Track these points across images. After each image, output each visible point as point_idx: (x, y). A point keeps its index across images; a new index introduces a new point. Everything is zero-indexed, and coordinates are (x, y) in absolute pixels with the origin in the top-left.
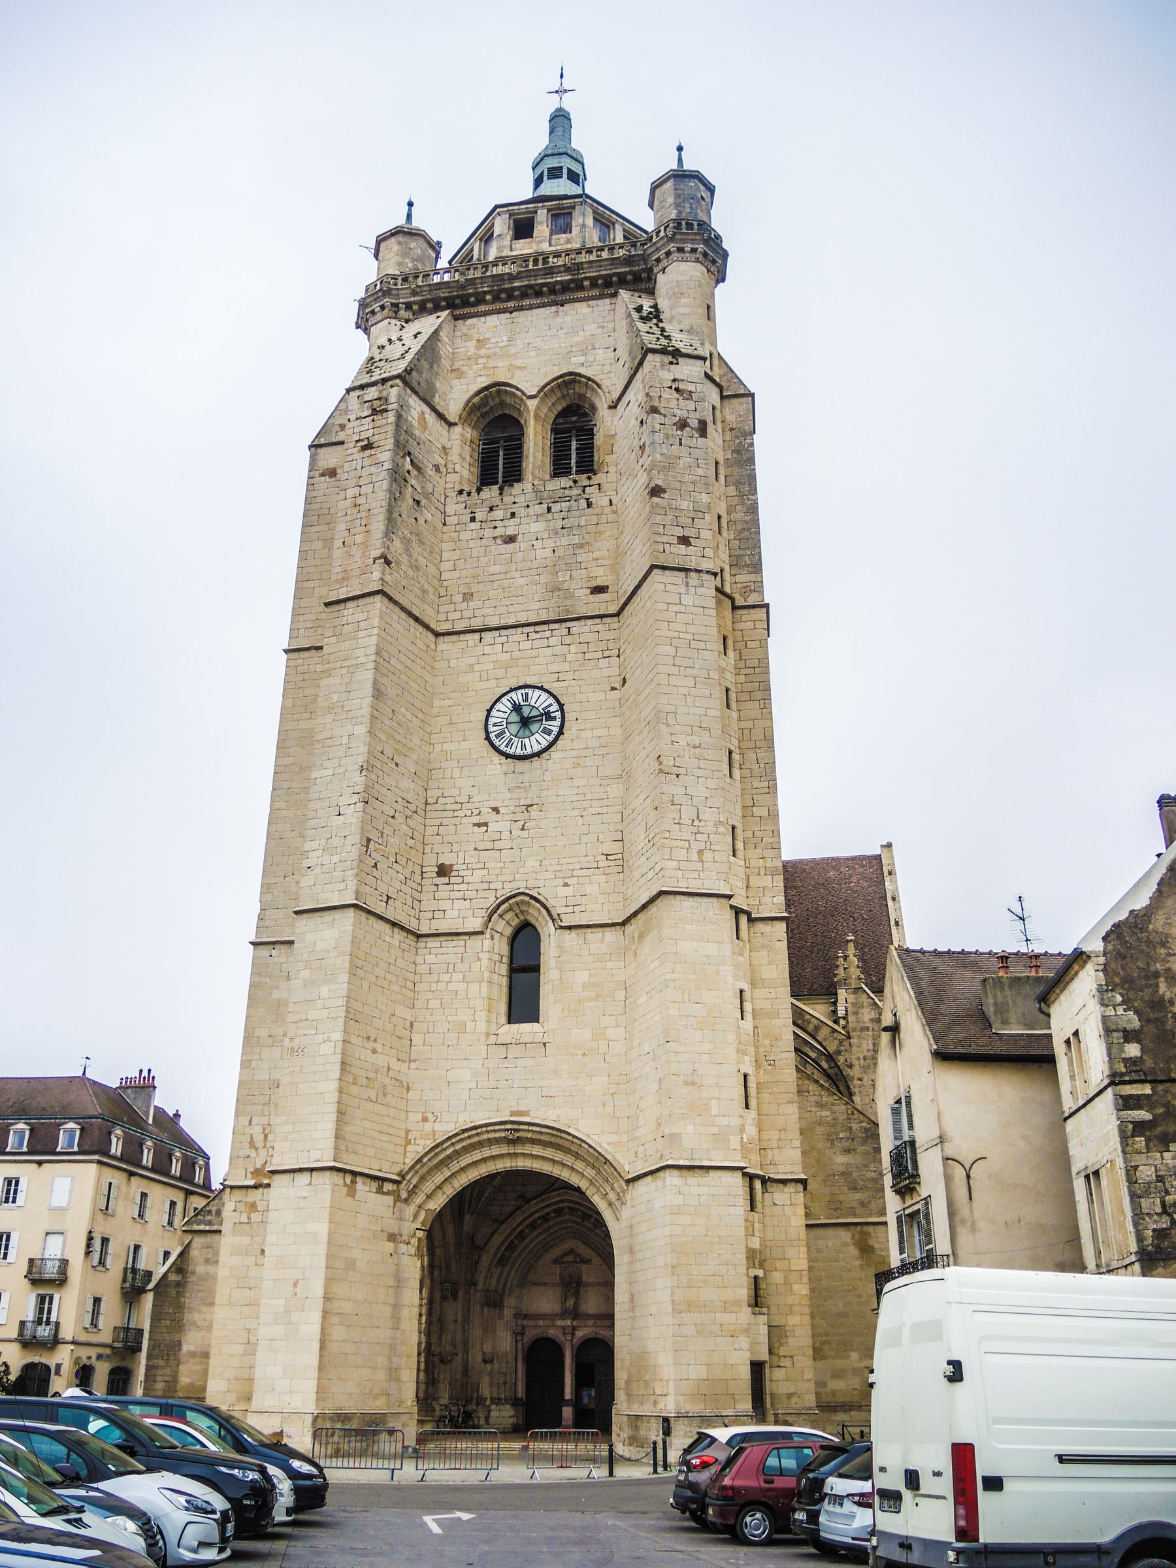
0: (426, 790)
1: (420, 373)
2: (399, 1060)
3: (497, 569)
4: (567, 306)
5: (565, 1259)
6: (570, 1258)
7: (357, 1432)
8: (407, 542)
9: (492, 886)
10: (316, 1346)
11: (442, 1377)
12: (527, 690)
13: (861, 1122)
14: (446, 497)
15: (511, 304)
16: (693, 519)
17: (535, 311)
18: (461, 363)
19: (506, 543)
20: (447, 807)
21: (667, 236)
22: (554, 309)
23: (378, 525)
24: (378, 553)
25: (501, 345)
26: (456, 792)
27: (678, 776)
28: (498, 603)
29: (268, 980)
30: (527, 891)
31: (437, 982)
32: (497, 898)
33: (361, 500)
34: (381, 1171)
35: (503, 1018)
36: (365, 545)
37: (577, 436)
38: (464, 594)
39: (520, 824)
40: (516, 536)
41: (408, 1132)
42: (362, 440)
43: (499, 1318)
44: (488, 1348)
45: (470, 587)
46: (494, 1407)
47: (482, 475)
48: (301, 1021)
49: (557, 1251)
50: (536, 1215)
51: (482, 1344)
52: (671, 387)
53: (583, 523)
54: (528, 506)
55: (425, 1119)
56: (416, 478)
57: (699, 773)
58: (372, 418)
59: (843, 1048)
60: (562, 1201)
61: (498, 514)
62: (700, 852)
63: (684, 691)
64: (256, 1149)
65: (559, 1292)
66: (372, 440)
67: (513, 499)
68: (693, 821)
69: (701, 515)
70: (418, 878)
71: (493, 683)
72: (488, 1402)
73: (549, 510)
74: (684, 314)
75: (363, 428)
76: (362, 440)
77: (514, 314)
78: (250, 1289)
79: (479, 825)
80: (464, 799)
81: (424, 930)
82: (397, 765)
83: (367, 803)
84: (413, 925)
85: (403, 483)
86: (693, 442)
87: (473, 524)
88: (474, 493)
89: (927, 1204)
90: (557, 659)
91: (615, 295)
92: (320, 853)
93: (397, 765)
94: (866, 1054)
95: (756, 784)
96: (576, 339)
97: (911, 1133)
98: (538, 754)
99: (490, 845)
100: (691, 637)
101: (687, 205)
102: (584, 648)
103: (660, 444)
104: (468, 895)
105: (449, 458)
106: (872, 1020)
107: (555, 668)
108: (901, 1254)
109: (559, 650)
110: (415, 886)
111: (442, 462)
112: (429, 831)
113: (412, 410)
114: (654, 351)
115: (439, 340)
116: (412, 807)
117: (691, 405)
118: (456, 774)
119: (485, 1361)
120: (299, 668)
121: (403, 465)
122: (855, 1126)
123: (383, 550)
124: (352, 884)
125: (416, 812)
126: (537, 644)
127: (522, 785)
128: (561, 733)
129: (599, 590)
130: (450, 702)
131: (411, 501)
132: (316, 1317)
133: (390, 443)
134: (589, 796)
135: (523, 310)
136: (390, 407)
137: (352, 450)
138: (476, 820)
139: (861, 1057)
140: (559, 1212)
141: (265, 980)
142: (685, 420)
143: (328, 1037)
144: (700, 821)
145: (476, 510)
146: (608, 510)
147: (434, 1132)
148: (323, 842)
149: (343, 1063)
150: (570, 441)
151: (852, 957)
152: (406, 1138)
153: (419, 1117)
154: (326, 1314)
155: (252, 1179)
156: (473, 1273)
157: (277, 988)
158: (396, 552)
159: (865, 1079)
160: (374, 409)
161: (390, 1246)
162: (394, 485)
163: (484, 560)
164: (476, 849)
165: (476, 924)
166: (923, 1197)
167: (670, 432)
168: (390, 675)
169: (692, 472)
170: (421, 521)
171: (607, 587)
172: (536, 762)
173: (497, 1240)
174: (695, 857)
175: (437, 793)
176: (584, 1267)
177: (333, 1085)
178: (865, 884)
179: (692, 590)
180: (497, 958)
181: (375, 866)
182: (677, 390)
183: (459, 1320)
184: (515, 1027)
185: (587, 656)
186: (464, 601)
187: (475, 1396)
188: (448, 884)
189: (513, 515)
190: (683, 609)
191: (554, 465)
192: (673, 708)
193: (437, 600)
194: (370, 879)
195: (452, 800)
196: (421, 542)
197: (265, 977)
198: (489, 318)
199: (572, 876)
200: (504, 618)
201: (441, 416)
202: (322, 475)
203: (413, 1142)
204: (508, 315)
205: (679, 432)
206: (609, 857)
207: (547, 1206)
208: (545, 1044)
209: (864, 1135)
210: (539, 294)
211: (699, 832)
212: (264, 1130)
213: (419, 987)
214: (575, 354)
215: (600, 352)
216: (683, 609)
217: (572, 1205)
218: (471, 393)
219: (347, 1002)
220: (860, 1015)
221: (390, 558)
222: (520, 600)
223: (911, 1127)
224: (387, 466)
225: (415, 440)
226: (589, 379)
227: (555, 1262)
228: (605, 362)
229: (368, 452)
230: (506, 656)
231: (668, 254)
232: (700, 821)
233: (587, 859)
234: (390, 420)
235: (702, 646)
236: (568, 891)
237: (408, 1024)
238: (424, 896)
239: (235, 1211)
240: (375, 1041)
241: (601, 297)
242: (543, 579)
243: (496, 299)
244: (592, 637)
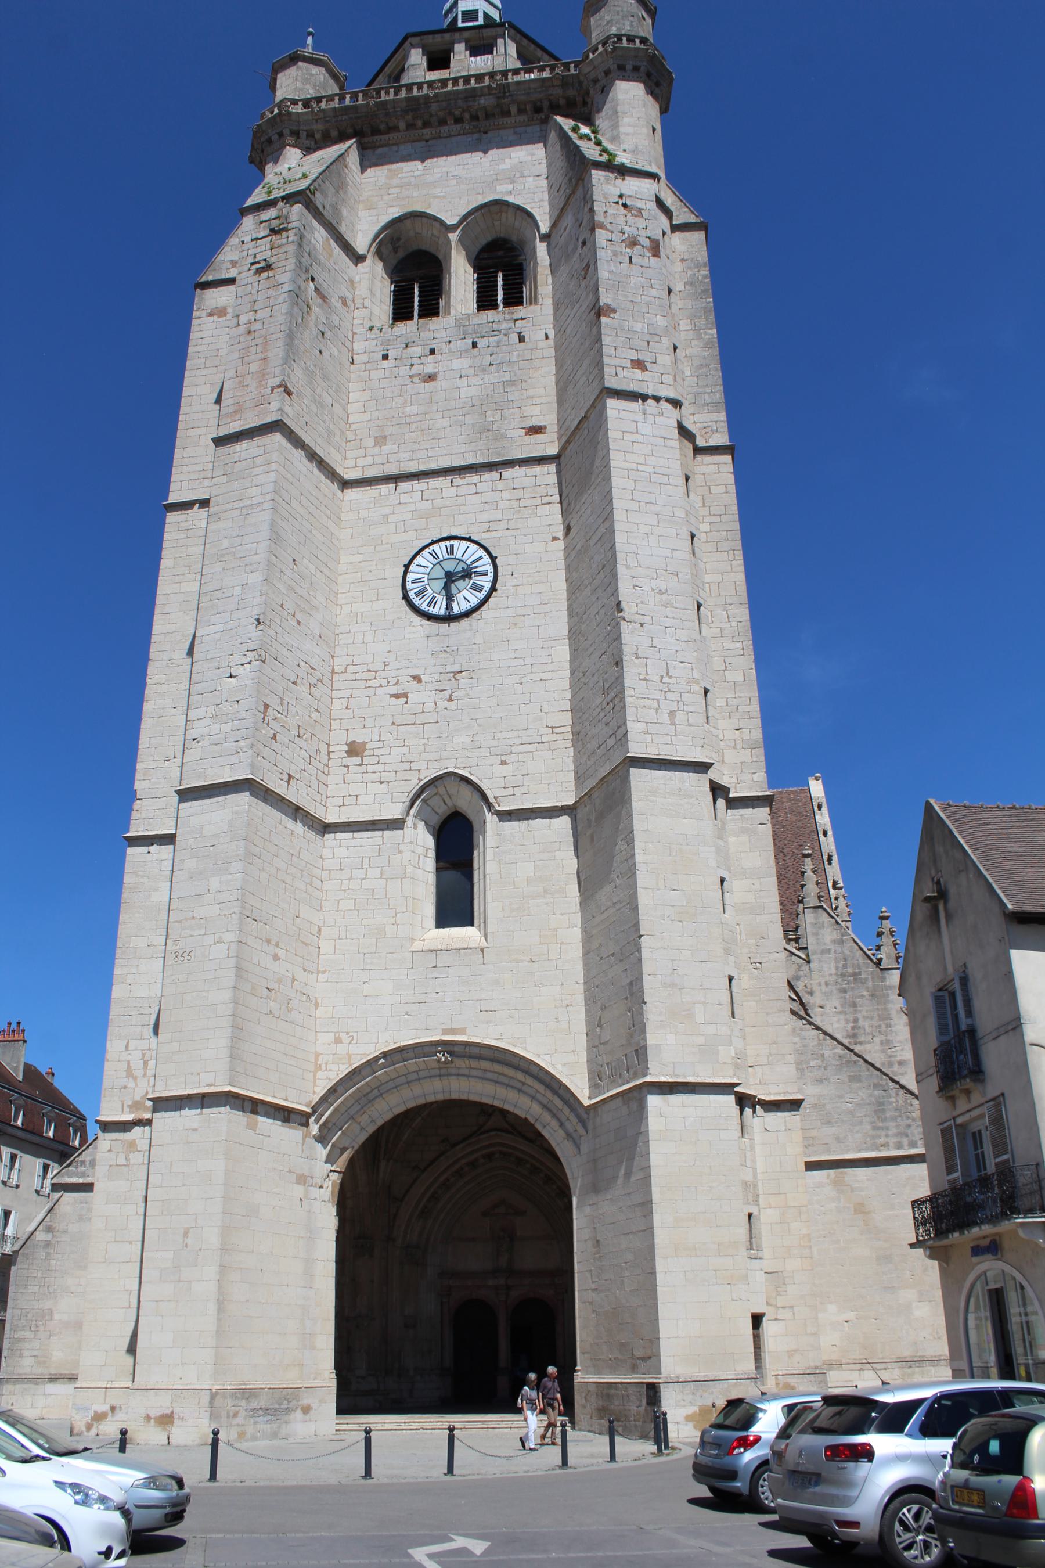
0: (333, 657)
1: (325, 196)
2: (305, 970)
3: (415, 409)
4: (490, 134)
7: (266, 1411)
8: (310, 375)
9: (414, 766)
10: (212, 1308)
12: (452, 542)
13: (833, 1049)
14: (354, 334)
16: (648, 342)
17: (454, 139)
18: (370, 193)
19: (425, 381)
20: (358, 676)
21: (606, 50)
22: (476, 136)
23: (277, 351)
24: (277, 381)
25: (416, 173)
26: (369, 659)
27: (642, 625)
28: (417, 447)
29: (145, 880)
30: (457, 771)
31: (350, 879)
32: (420, 780)
34: (286, 1100)
35: (431, 921)
36: (262, 375)
37: (502, 271)
38: (376, 437)
39: (447, 694)
41: (317, 1055)
42: (258, 263)
45: (383, 430)
47: (394, 314)
48: (186, 919)
50: (464, 1161)
52: (617, 203)
53: (514, 359)
54: (450, 342)
55: (338, 1041)
56: (320, 306)
57: (668, 622)
58: (270, 238)
59: (801, 973)
61: (416, 350)
62: (672, 714)
63: (647, 530)
64: (135, 1078)
67: (431, 335)
68: (662, 677)
69: (657, 338)
70: (324, 758)
71: (411, 535)
73: (475, 345)
74: (628, 134)
75: (259, 249)
76: (258, 263)
77: (430, 142)
78: (131, 1243)
79: (397, 696)
80: (378, 666)
81: (331, 819)
82: (299, 623)
83: (264, 662)
84: (319, 812)
85: (306, 309)
86: (645, 262)
87: (386, 361)
88: (386, 329)
89: (999, 1105)
90: (487, 507)
91: (546, 121)
92: (207, 722)
93: (299, 623)
94: (827, 978)
95: (727, 645)
96: (502, 167)
97: (969, 1021)
98: (467, 614)
99: (410, 719)
100: (652, 471)
102: (519, 494)
103: (607, 261)
104: (385, 777)
105: (357, 293)
106: (834, 942)
107: (485, 517)
108: (948, 1174)
109: (489, 497)
110: (321, 766)
111: (351, 296)
112: (337, 704)
113: (316, 233)
114: (598, 165)
115: (346, 167)
116: (318, 675)
117: (641, 223)
118: (369, 638)
120: (182, 524)
121: (306, 289)
122: (827, 1053)
123: (282, 378)
124: (246, 757)
125: (320, 680)
126: (463, 490)
127: (448, 649)
128: (493, 589)
129: (536, 430)
130: (360, 558)
131: (315, 331)
132: (211, 1272)
133: (291, 264)
134: (529, 661)
135: (440, 137)
136: (290, 226)
137: (246, 277)
138: (394, 690)
139: (823, 981)
140: (489, 1157)
141: (142, 880)
142: (636, 238)
143: (220, 938)
144: (671, 677)
145: (389, 347)
147: (349, 1056)
148: (211, 709)
149: (238, 968)
150: (496, 277)
151: (809, 873)
152: (316, 1063)
153: (331, 1037)
154: (223, 1268)
155: (131, 1112)
157: (156, 890)
158: (298, 382)
159: (827, 1007)
161: (299, 1190)
162: (296, 309)
163: (399, 401)
164: (393, 724)
165: (394, 811)
166: (990, 1096)
167: (619, 249)
168: (291, 519)
169: (645, 293)
170: (326, 353)
171: (545, 427)
172: (464, 623)
174: (665, 719)
175: (347, 660)
177: (227, 995)
178: (794, 818)
179: (651, 418)
180: (420, 850)
181: (274, 737)
182: (625, 206)
184: (441, 930)
185: (523, 503)
186: (375, 445)
188: (360, 765)
190: (640, 438)
191: (478, 302)
192: (633, 548)
193: (344, 445)
194: (267, 752)
195: (365, 668)
196: (325, 377)
197: (143, 877)
198: (402, 147)
199: (511, 753)
200: (424, 463)
201: (347, 247)
202: (211, 314)
205: (628, 250)
206: (556, 730)
208: (482, 950)
209: (838, 1063)
210: (458, 120)
211: (669, 691)
212: (144, 1055)
213: (327, 886)
214: (501, 182)
215: (531, 179)
216: (640, 438)
217: (504, 1149)
218: (382, 224)
219: (243, 895)
220: (820, 937)
221: (290, 387)
222: (442, 442)
223: (969, 1013)
224: (286, 288)
225: (320, 265)
226: (519, 209)
229: (264, 275)
230: (427, 505)
231: (607, 73)
232: (671, 677)
233: (529, 733)
234: (290, 239)
235: (665, 480)
236: (507, 770)
237: (315, 931)
238: (330, 780)
239: (110, 1151)
240: (277, 945)
242: (469, 420)
243: (411, 126)
244: (528, 482)
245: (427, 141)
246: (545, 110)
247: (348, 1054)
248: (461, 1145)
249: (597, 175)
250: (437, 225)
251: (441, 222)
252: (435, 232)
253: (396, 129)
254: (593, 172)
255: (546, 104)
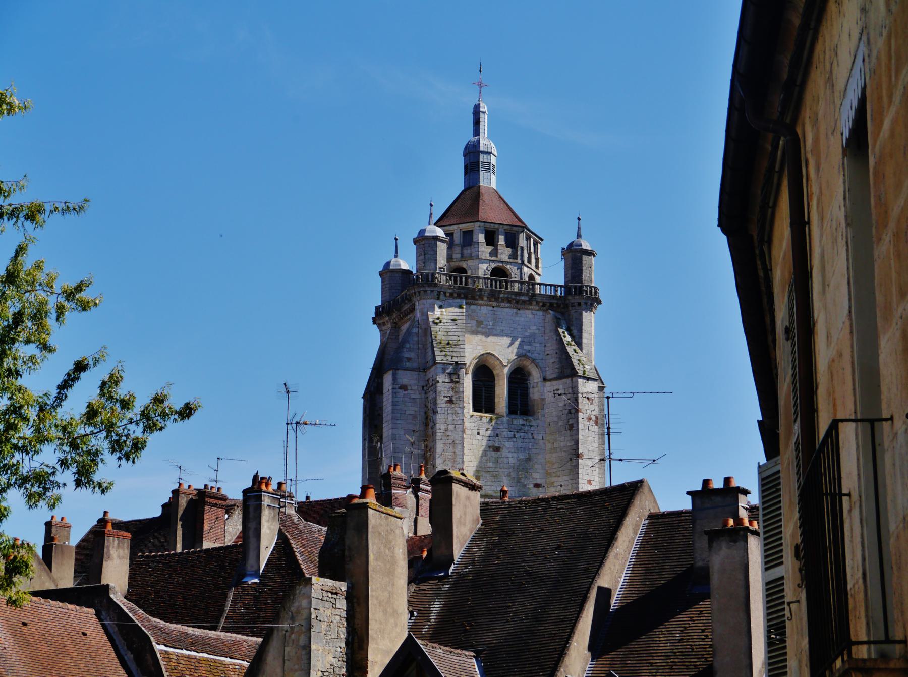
4: (521, 312)
15: (494, 304)
19: (494, 450)
22: (515, 310)
25: (489, 327)
33: (449, 433)
40: (499, 447)
42: (447, 397)
66: (454, 398)
77: (495, 309)
101: (588, 272)
114: (580, 377)
146: (541, 442)
160: (452, 380)
182: (588, 398)
189: (497, 435)
202: (400, 388)
204: (492, 308)
210: (509, 302)
228: (541, 352)
241: (540, 309)
245: (493, 307)
246: (547, 306)
249: (580, 381)
250: (499, 362)
251: (501, 362)
252: (496, 363)
253: (482, 300)
254: (579, 380)
255: (548, 304)
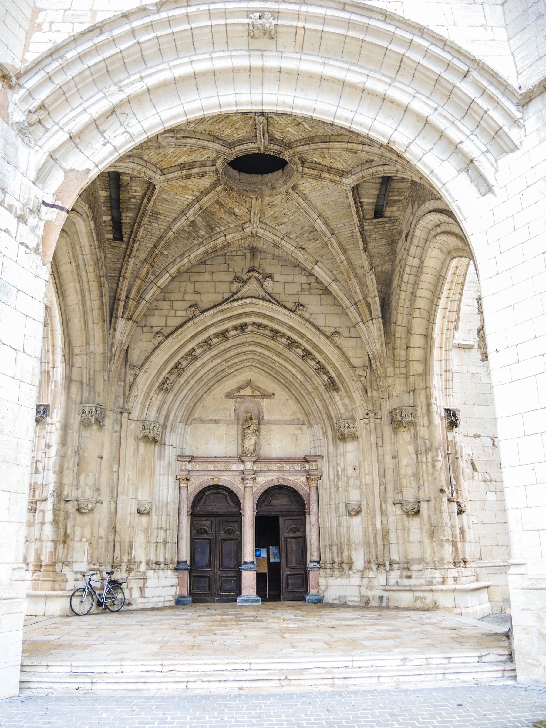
5: (242, 392)
6: (248, 391)
11: (78, 533)
43: (160, 458)
44: (143, 496)
46: (150, 573)
49: (231, 384)
50: (213, 331)
51: (136, 491)
60: (247, 314)
65: (234, 431)
72: (143, 567)
119: (139, 512)
140: (242, 328)
156: (126, 397)
173: (158, 359)
176: (265, 403)
183: (105, 457)
187: (125, 558)
203: (46, 27)
207: (229, 319)
227: (229, 395)
247: (91, 10)
248: (211, 312)
